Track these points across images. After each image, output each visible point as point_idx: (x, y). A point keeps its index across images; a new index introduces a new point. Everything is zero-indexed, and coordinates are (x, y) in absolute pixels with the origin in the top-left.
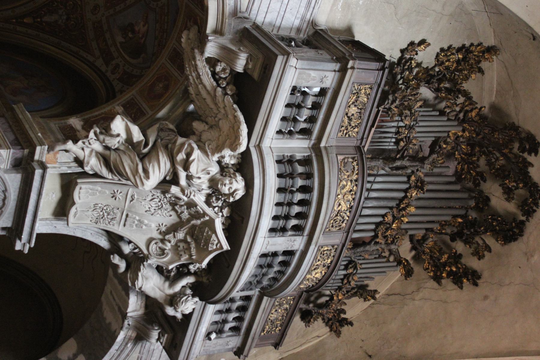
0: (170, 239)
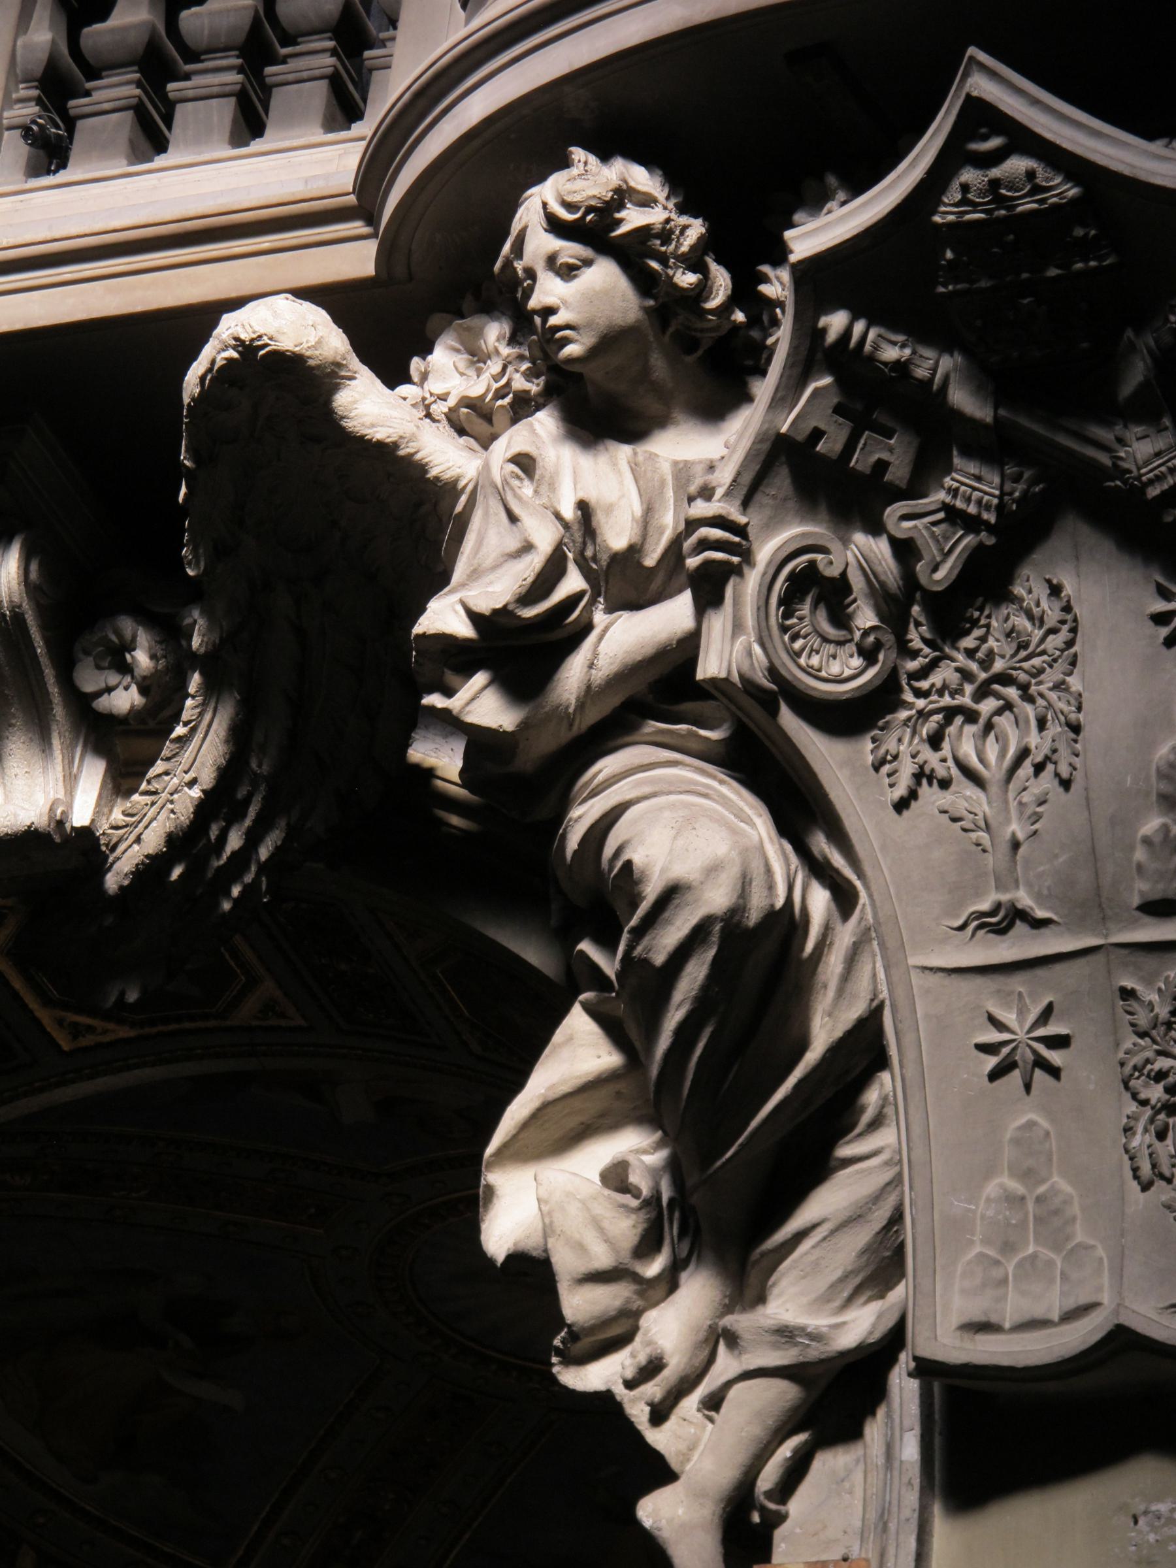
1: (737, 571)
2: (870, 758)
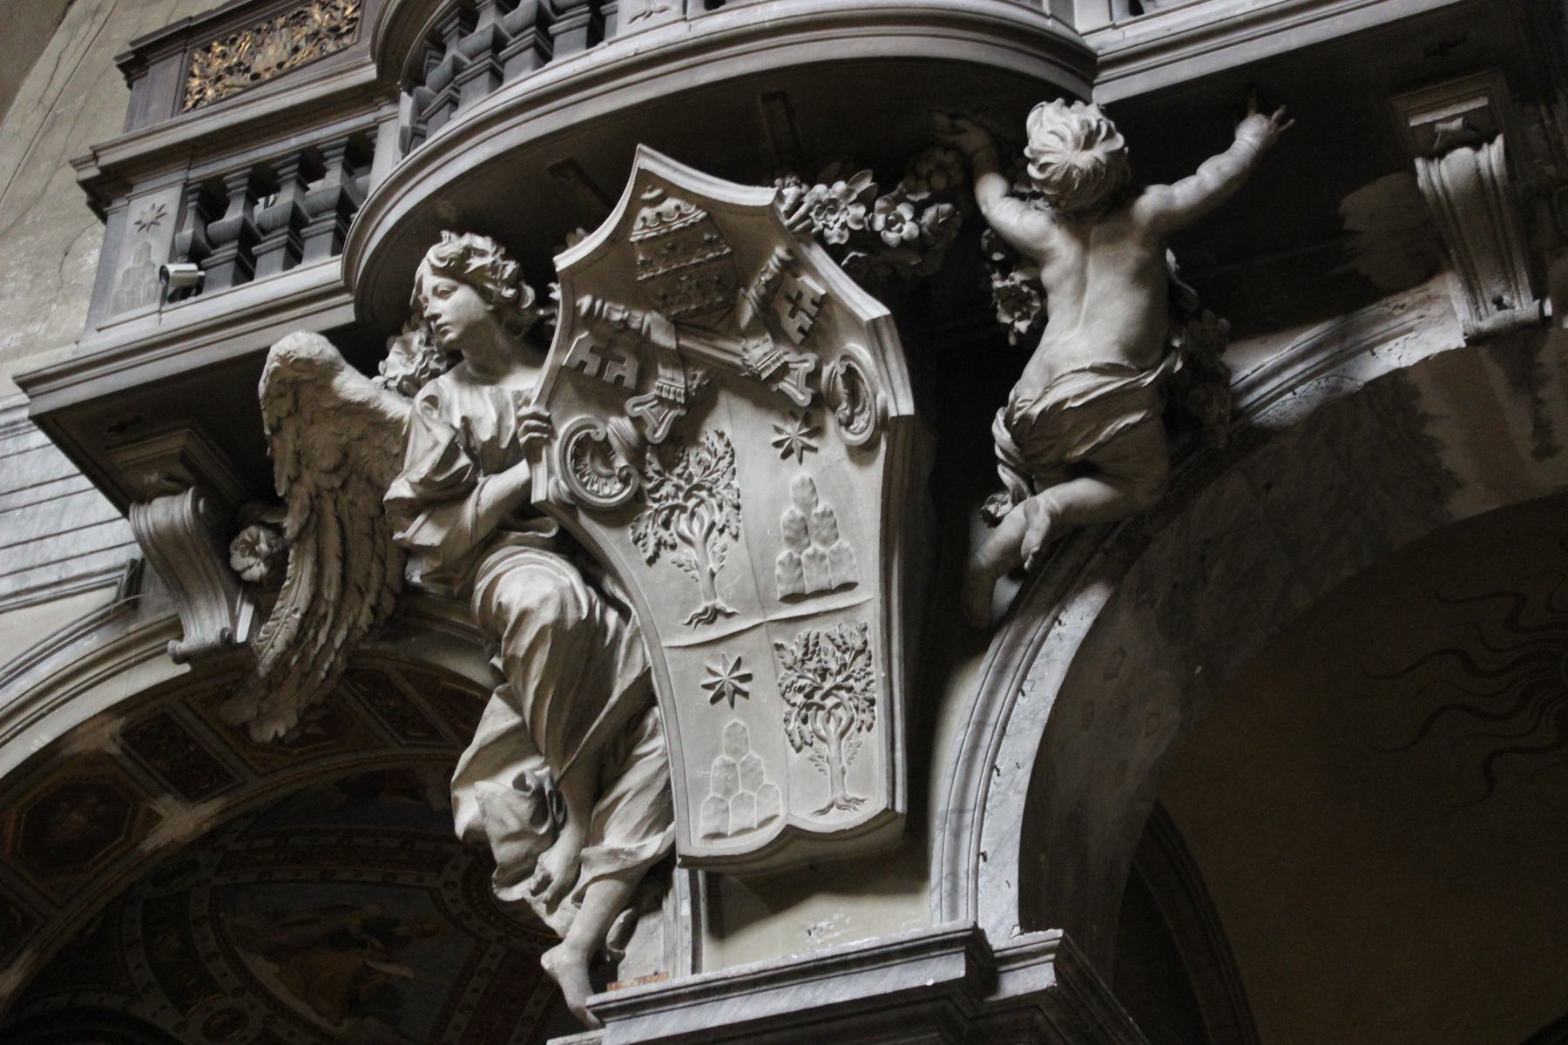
0: (802, 381)
1: (548, 442)
2: (631, 538)
